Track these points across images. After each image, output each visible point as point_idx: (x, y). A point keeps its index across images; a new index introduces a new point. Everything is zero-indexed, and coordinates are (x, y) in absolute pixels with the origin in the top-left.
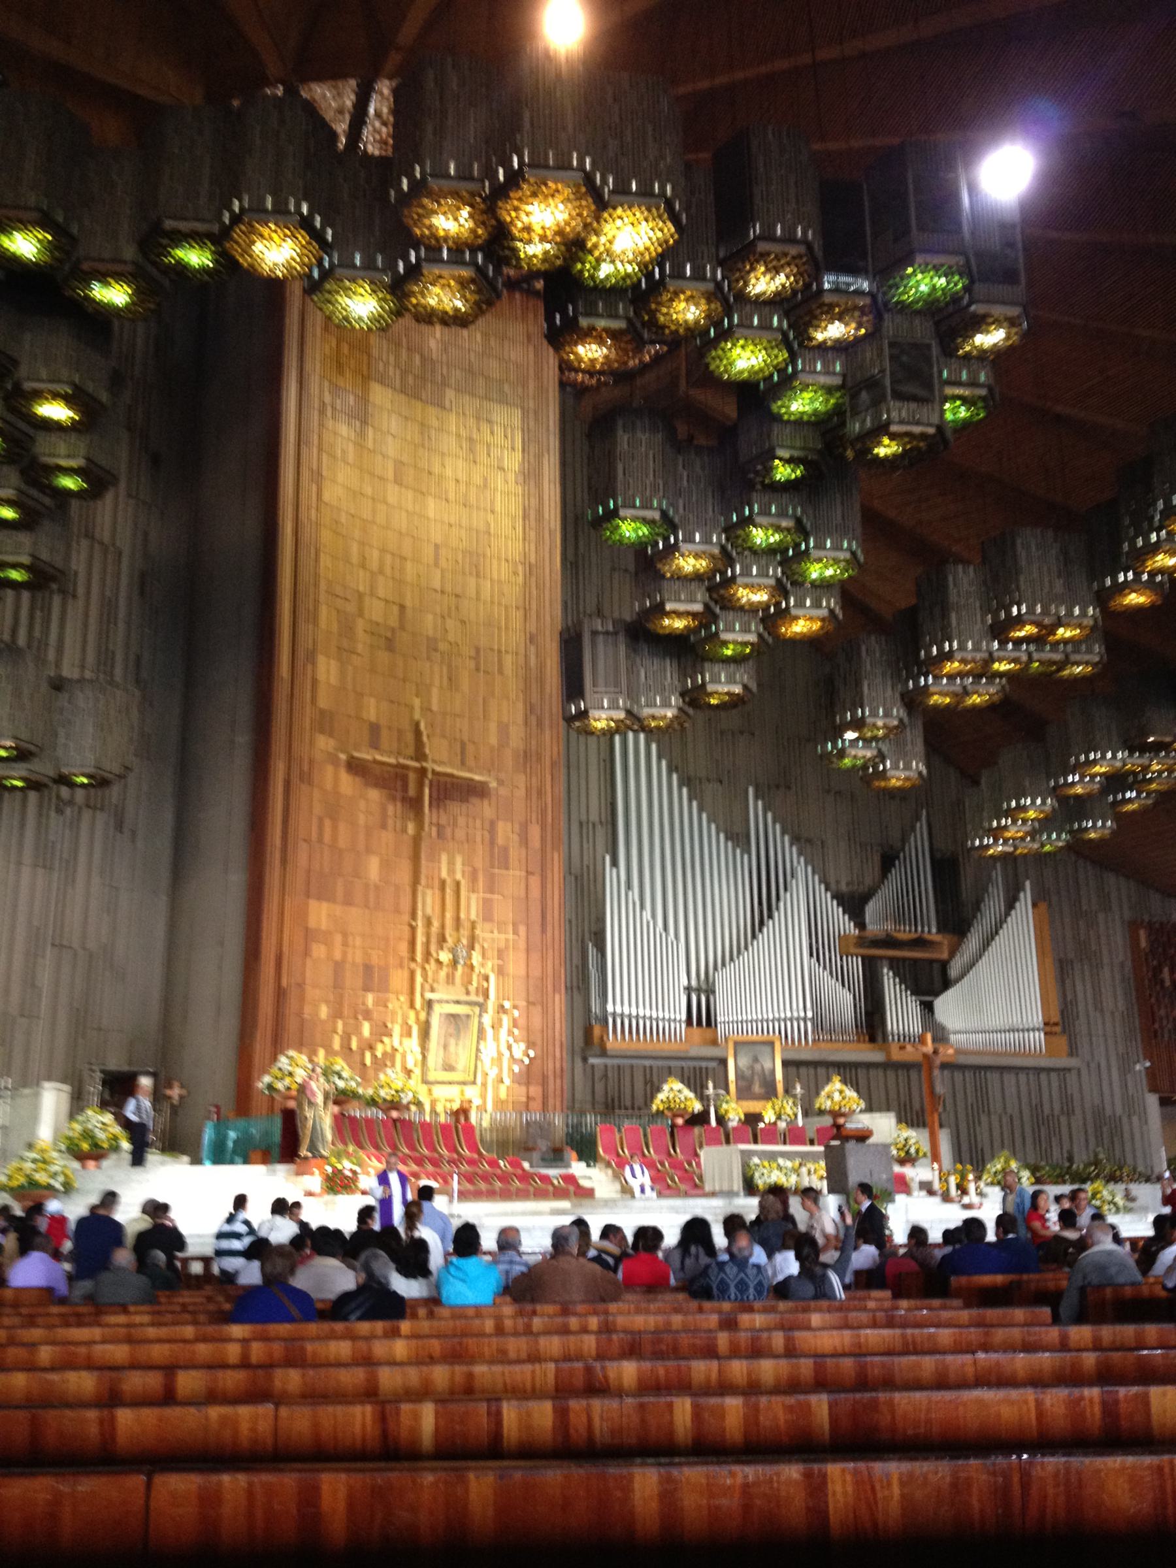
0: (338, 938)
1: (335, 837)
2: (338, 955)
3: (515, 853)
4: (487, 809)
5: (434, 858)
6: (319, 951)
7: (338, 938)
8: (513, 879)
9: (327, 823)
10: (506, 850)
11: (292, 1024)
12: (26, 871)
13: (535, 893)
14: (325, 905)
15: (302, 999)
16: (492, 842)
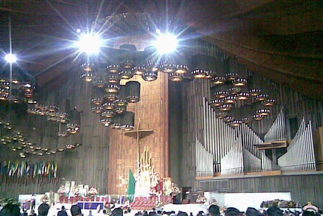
0: (123, 165)
1: (122, 147)
2: (123, 168)
3: (158, 143)
4: (153, 136)
5: (143, 147)
6: (120, 167)
7: (123, 165)
8: (158, 149)
9: (120, 146)
10: (156, 143)
11: (114, 181)
12: (95, 160)
13: (162, 151)
14: (120, 160)
15: (116, 176)
16: (154, 141)
